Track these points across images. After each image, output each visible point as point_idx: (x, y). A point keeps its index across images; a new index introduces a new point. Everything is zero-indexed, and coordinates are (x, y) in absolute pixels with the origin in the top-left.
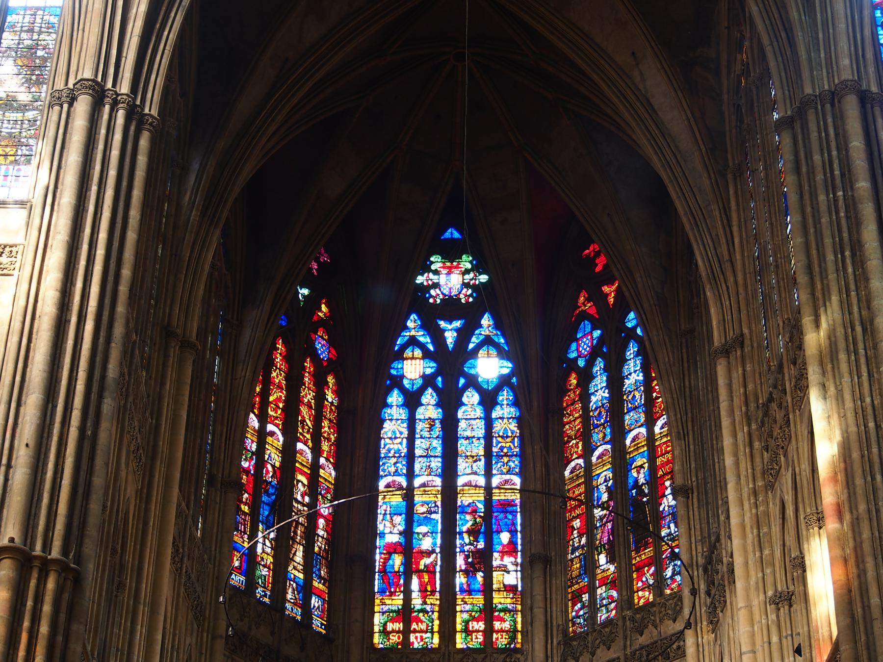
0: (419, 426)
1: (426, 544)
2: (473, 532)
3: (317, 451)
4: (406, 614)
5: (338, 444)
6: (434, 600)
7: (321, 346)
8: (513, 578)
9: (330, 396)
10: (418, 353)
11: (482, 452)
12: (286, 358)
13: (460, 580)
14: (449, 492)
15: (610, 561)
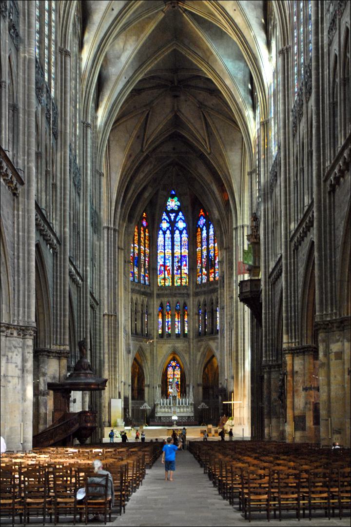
0: (166, 239)
1: (168, 264)
2: (178, 262)
3: (145, 247)
4: (164, 279)
5: (149, 244)
6: (170, 276)
7: (144, 223)
8: (186, 271)
9: (147, 234)
10: (165, 221)
11: (179, 244)
12: (138, 229)
13: (175, 272)
14: (173, 253)
15: (206, 270)
